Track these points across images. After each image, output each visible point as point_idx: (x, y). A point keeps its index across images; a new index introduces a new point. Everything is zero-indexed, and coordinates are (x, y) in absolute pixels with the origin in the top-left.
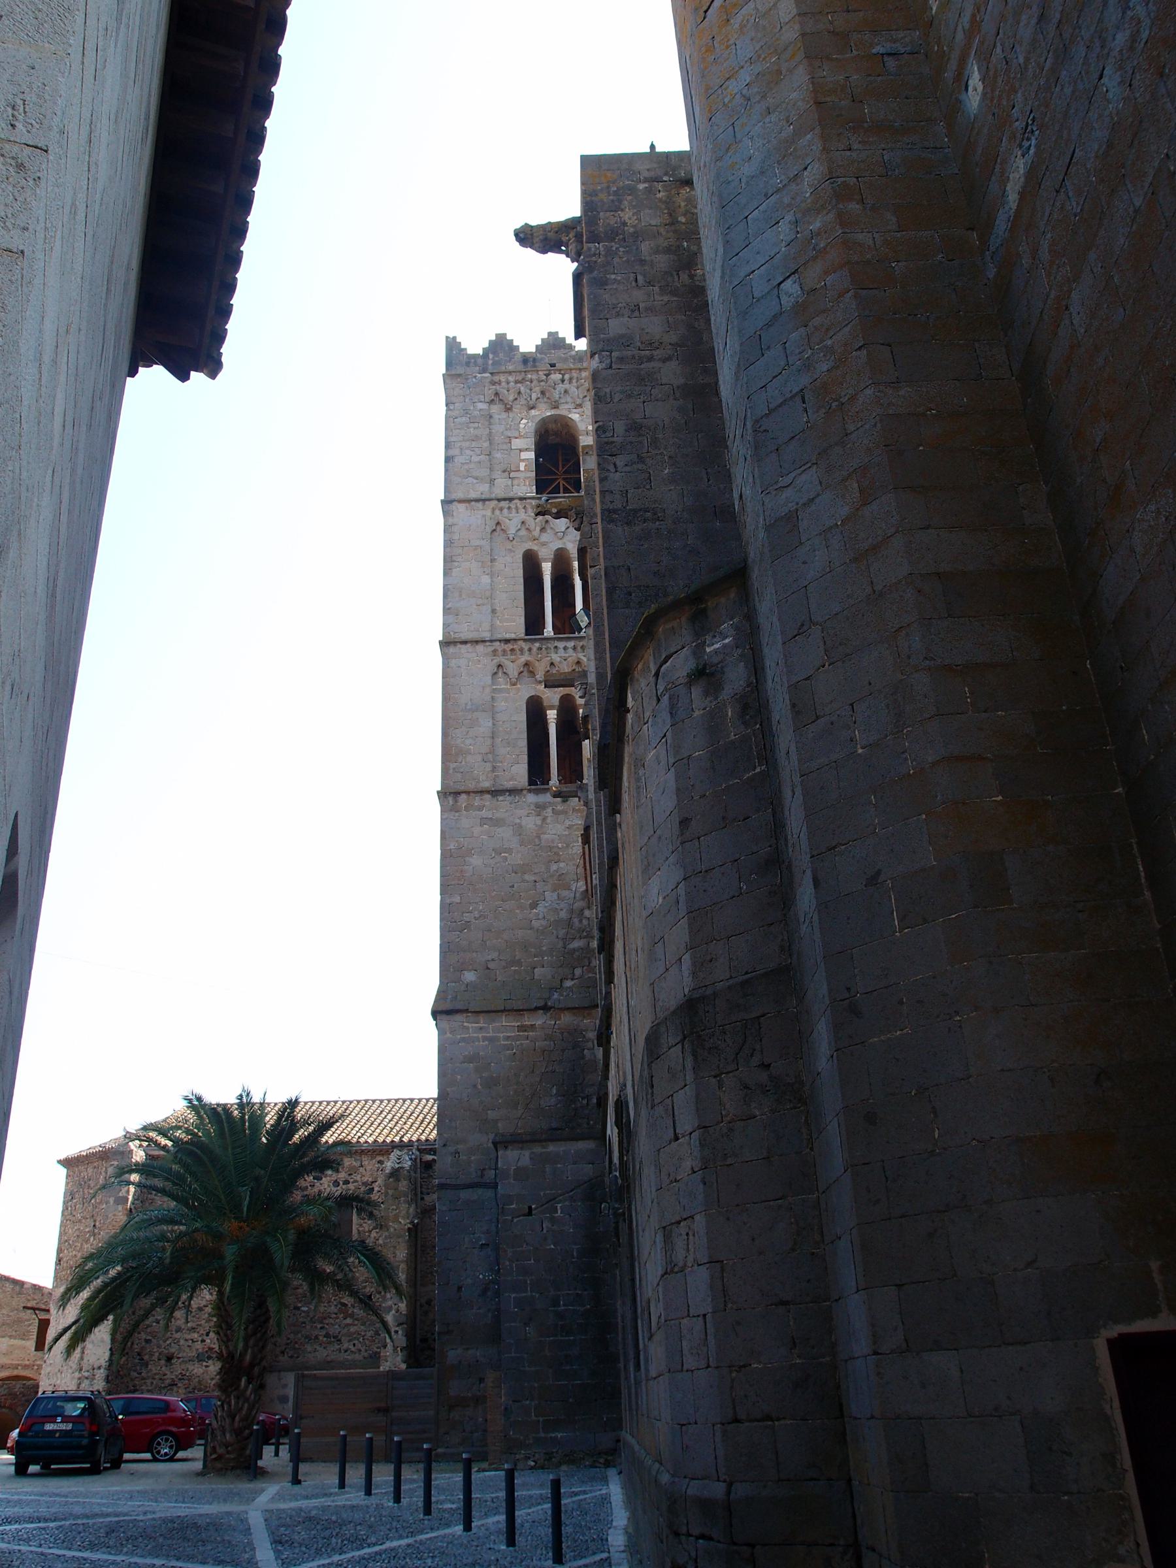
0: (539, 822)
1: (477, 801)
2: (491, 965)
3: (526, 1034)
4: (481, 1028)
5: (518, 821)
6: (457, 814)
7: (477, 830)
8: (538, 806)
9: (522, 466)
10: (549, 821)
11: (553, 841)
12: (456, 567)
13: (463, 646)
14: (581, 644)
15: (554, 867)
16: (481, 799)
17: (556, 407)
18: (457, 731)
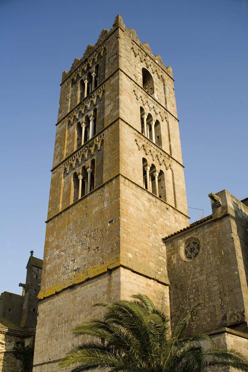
0: (149, 205)
1: (131, 184)
2: (137, 254)
3: (148, 287)
4: (135, 279)
5: (143, 201)
6: (125, 186)
7: (132, 197)
8: (149, 199)
9: (139, 78)
10: (152, 206)
11: (153, 215)
12: (123, 95)
13: (126, 125)
14: (158, 150)
15: (154, 225)
16: (132, 186)
17: (148, 68)
18: (125, 154)
